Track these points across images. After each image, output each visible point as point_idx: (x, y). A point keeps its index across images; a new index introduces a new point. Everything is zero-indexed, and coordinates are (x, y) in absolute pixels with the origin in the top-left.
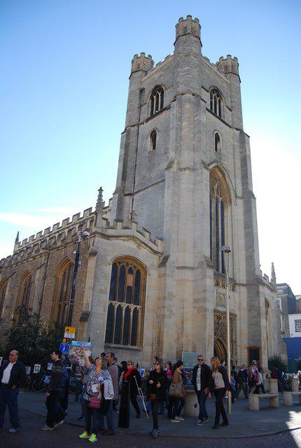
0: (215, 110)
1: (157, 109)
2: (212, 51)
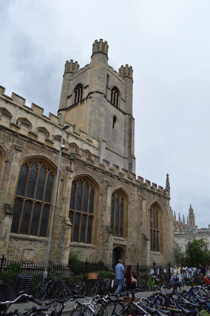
0: (115, 103)
1: (78, 100)
2: (115, 61)
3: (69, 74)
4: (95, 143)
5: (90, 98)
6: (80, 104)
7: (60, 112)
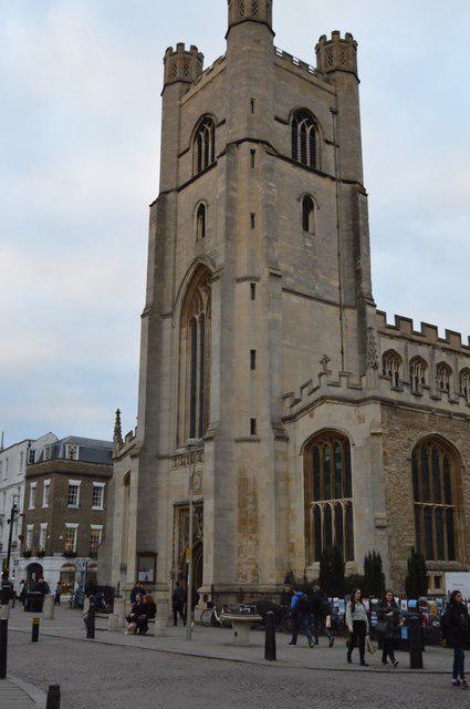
0: (304, 157)
1: (206, 161)
2: (296, 36)
3: (178, 85)
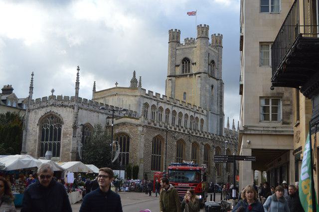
4: (205, 111)
5: (199, 77)
6: (188, 76)
7: (170, 78)
